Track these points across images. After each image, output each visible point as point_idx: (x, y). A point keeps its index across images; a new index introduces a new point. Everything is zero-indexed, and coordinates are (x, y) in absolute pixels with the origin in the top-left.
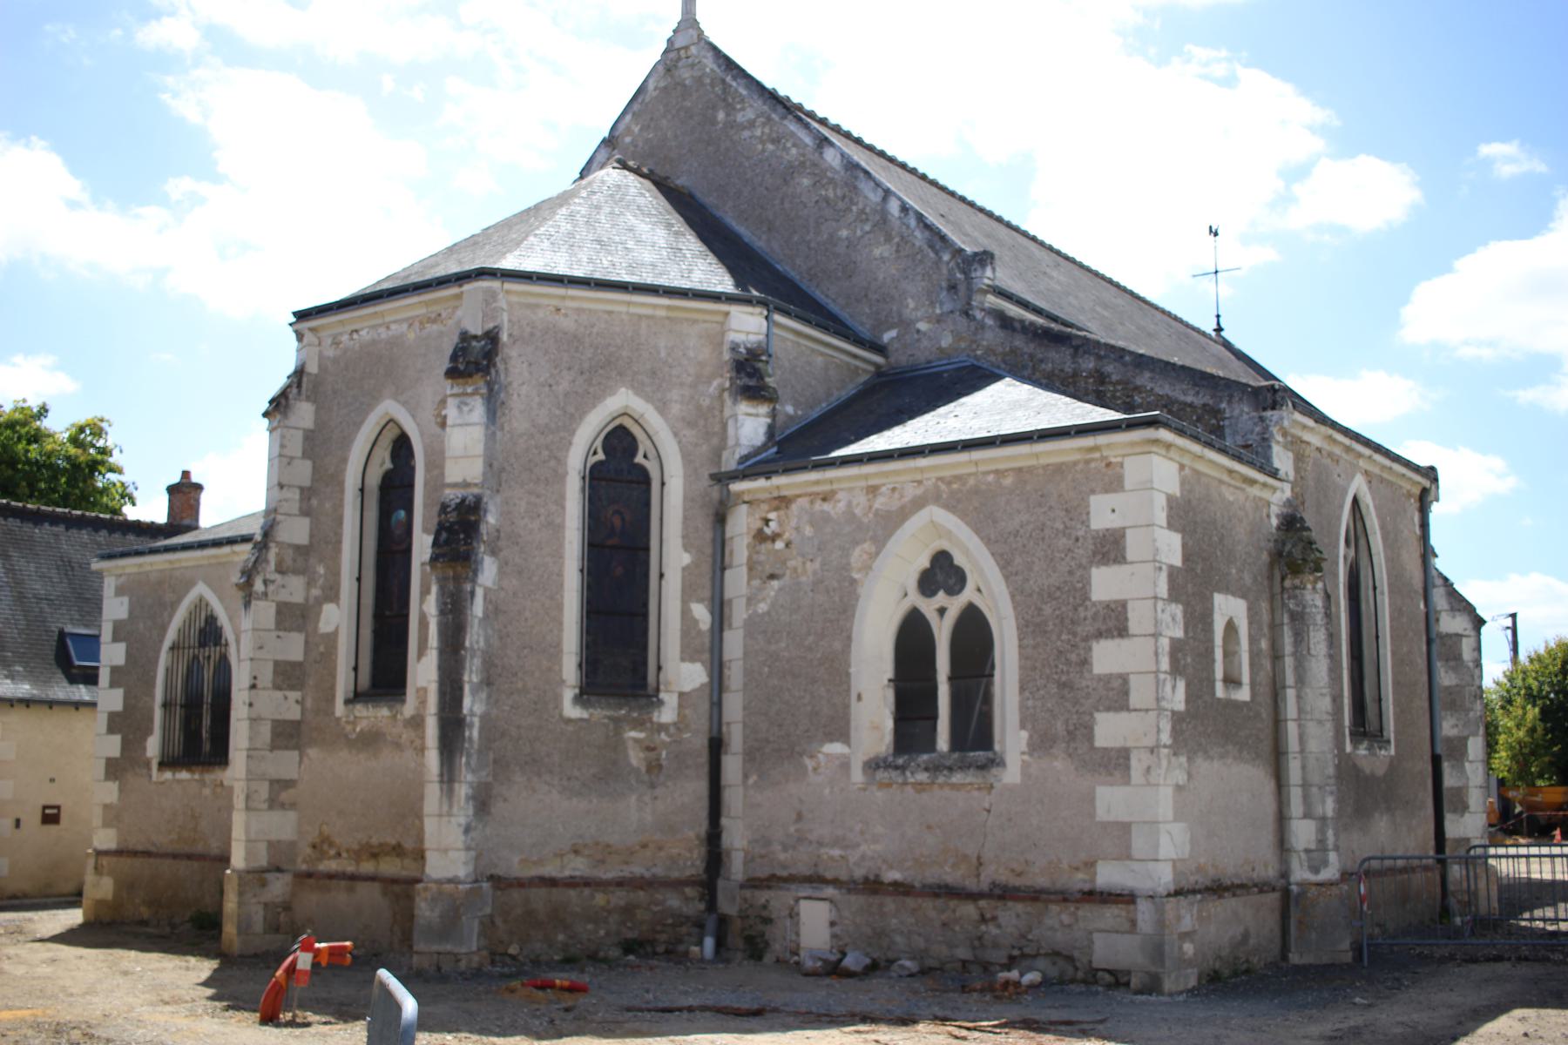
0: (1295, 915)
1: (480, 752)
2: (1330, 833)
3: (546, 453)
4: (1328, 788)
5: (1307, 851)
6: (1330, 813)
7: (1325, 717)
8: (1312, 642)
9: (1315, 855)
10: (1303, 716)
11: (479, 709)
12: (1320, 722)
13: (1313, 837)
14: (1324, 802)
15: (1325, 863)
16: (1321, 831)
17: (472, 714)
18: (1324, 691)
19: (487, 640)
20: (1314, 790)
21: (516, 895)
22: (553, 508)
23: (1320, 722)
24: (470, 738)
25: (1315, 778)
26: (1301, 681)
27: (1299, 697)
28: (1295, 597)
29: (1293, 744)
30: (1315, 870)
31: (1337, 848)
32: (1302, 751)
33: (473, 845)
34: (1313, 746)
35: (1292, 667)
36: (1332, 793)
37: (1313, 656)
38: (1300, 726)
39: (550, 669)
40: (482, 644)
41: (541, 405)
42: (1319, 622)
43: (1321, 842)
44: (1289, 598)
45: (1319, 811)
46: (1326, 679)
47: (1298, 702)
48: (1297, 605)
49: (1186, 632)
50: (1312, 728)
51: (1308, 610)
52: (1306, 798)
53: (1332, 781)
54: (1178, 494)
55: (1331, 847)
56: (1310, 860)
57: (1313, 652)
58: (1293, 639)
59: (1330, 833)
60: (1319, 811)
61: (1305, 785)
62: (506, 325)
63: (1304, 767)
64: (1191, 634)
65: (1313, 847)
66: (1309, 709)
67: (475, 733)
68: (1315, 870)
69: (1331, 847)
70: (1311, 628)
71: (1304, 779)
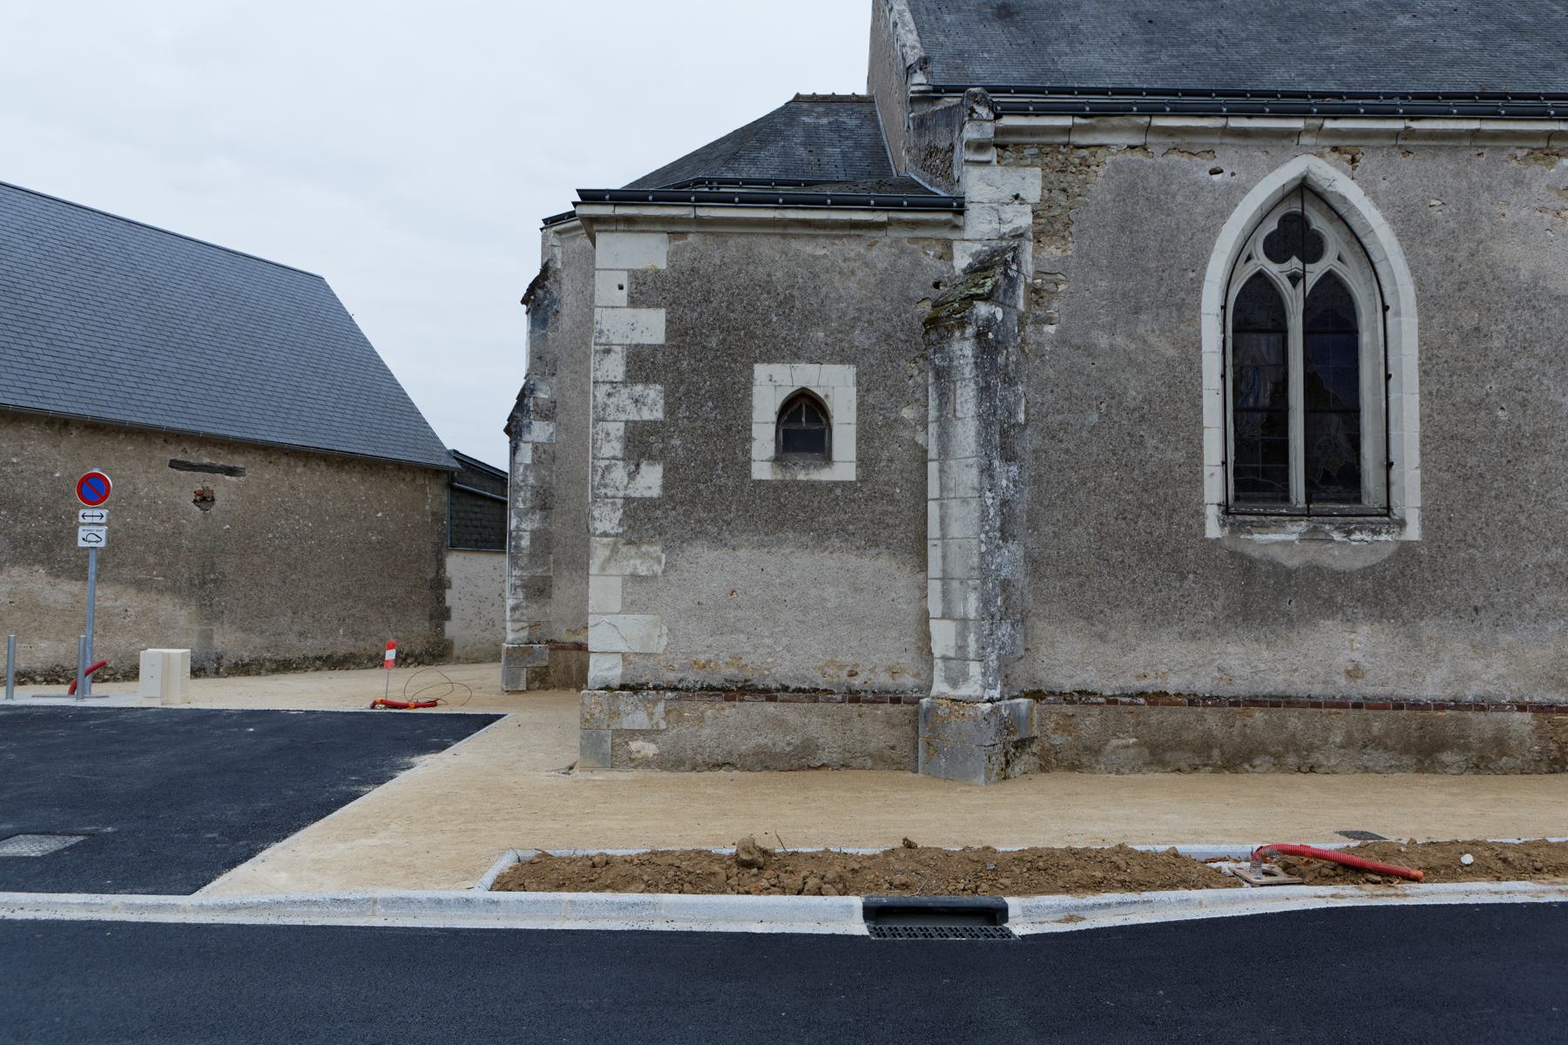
0: (924, 733)
1: (532, 555)
2: (972, 638)
3: (580, 341)
4: (970, 582)
5: (945, 658)
6: (972, 615)
7: (971, 493)
8: (958, 401)
9: (953, 664)
10: (945, 495)
11: (527, 526)
12: (964, 500)
13: (953, 643)
14: (966, 599)
15: (965, 676)
16: (962, 635)
17: (518, 529)
18: (971, 461)
19: (538, 477)
20: (955, 584)
21: (561, 654)
22: (584, 379)
23: (964, 500)
24: (516, 547)
25: (957, 570)
26: (944, 452)
27: (942, 471)
28: (942, 350)
29: (933, 530)
30: (954, 684)
31: (981, 659)
32: (943, 537)
33: (524, 618)
34: (955, 530)
35: (935, 436)
36: (976, 589)
37: (959, 419)
38: (941, 506)
39: (582, 496)
40: (531, 480)
41: (577, 307)
42: (967, 376)
43: (962, 648)
44: (935, 353)
45: (959, 610)
46: (973, 446)
47: (941, 478)
48: (943, 359)
49: (670, 410)
50: (955, 508)
51: (955, 363)
52: (945, 593)
53: (976, 573)
54: (662, 265)
55: (972, 655)
56: (947, 669)
57: (959, 414)
58: (937, 402)
59: (972, 638)
60: (959, 610)
61: (945, 579)
62: (559, 256)
63: (944, 557)
64: (682, 412)
65: (952, 654)
66: (952, 485)
67: (525, 543)
68: (954, 684)
69: (972, 655)
70: (958, 384)
71: (944, 571)
